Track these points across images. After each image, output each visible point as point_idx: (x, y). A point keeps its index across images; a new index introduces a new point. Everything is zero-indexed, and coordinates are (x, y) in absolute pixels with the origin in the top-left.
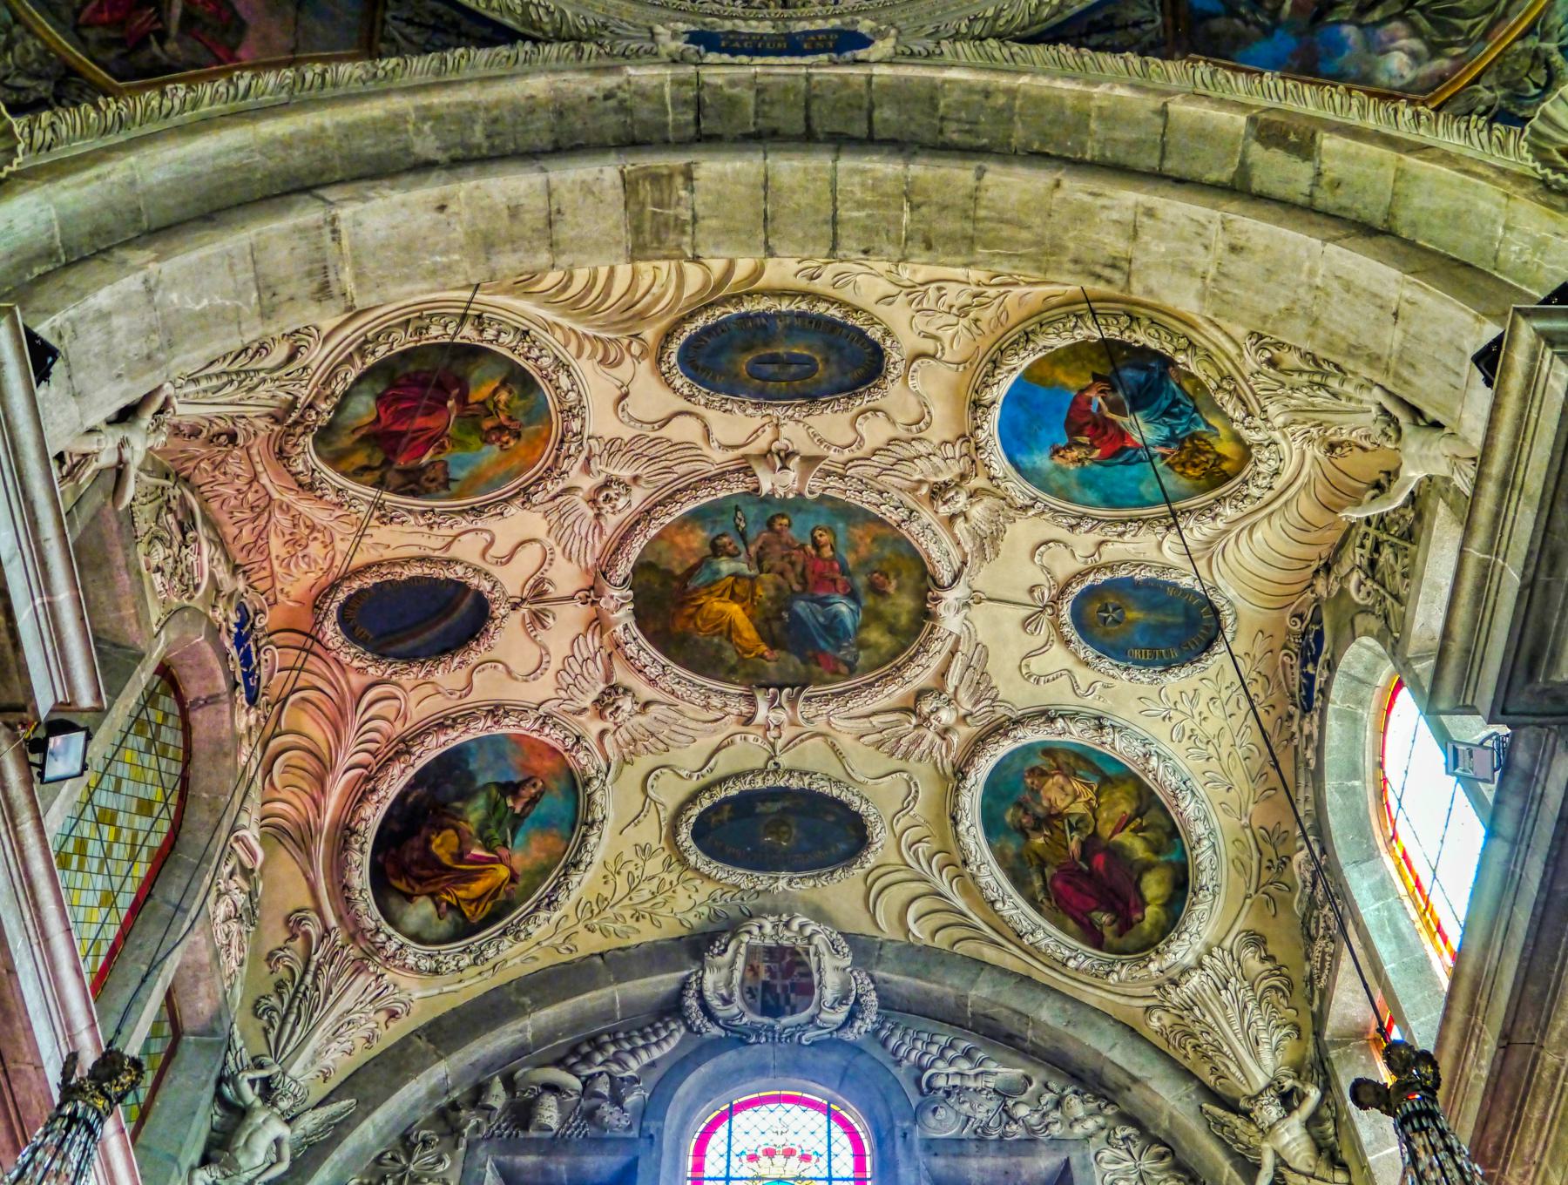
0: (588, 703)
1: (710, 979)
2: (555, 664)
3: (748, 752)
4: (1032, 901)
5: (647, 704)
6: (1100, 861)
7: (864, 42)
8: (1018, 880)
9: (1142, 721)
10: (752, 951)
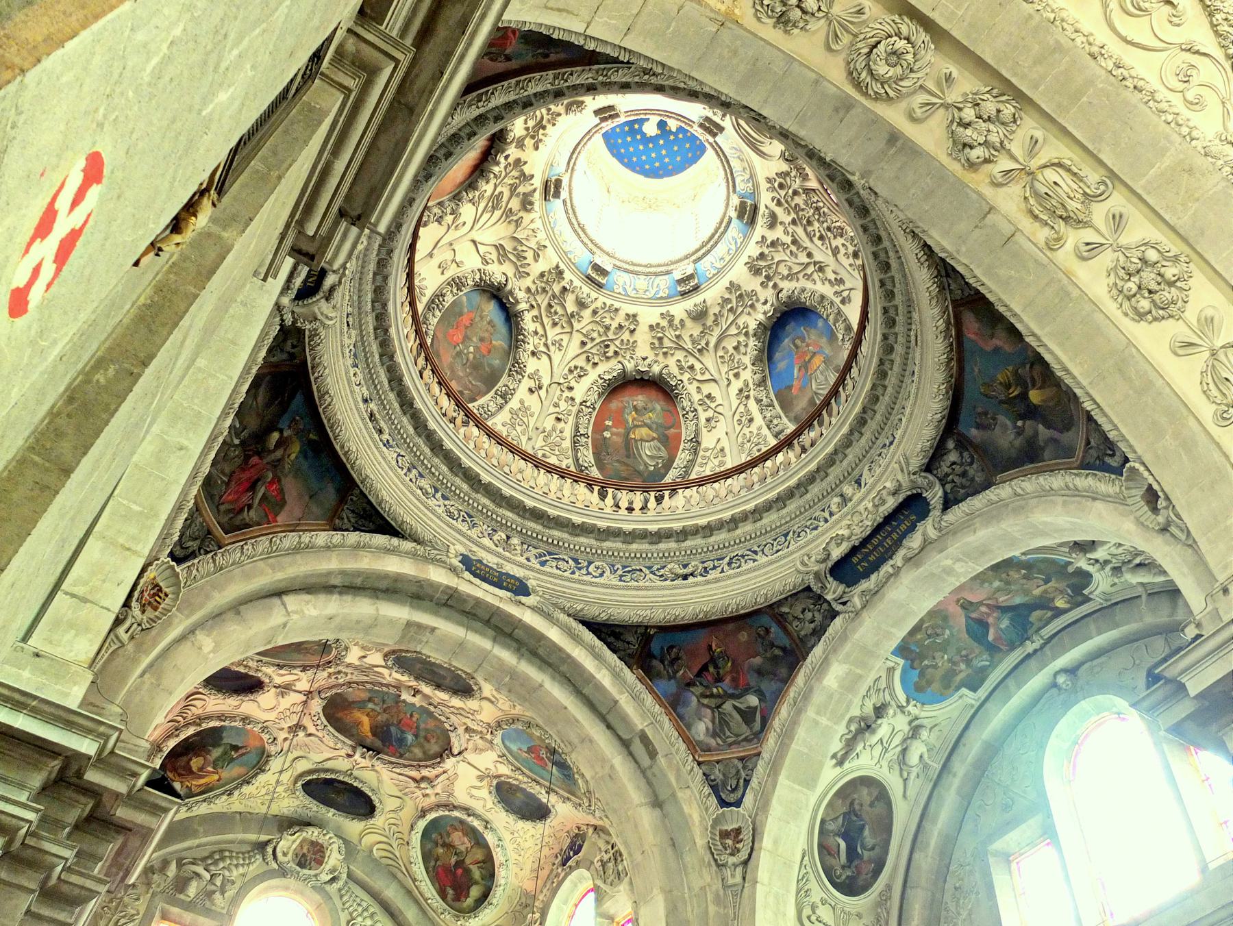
0: (286, 726)
2: (281, 709)
3: (343, 764)
4: (427, 869)
5: (310, 735)
6: (460, 871)
7: (527, 593)
8: (426, 857)
9: (503, 830)
10: (304, 840)
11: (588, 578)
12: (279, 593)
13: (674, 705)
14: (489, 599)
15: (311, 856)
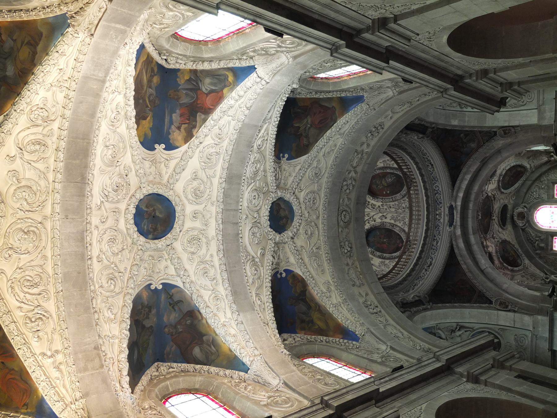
1: (521, 225)
3: (496, 220)
10: (518, 220)
11: (440, 189)
12: (482, 271)
13: (469, 155)
14: (459, 216)
15: (522, 216)
